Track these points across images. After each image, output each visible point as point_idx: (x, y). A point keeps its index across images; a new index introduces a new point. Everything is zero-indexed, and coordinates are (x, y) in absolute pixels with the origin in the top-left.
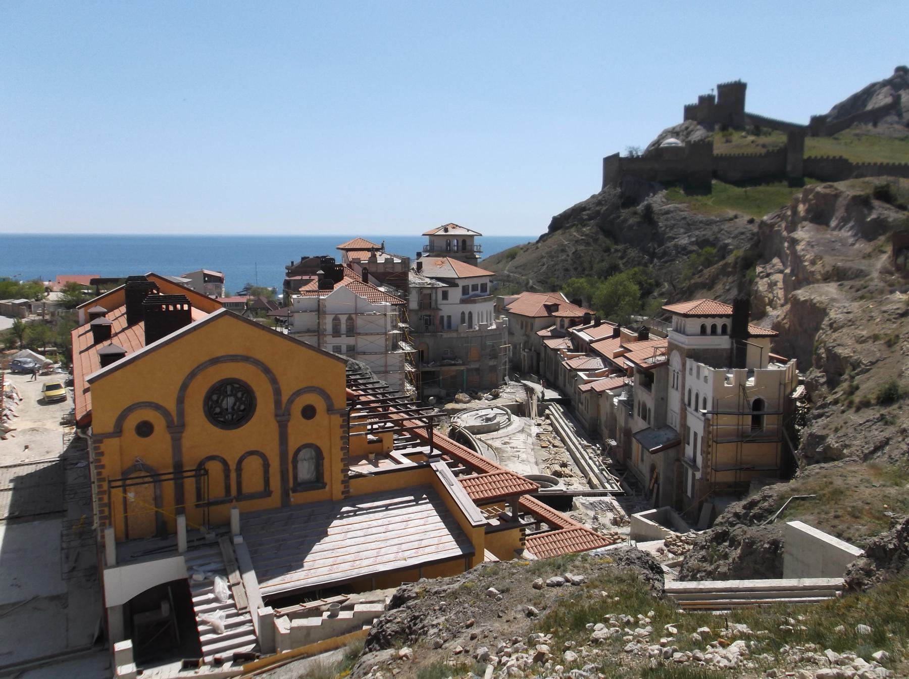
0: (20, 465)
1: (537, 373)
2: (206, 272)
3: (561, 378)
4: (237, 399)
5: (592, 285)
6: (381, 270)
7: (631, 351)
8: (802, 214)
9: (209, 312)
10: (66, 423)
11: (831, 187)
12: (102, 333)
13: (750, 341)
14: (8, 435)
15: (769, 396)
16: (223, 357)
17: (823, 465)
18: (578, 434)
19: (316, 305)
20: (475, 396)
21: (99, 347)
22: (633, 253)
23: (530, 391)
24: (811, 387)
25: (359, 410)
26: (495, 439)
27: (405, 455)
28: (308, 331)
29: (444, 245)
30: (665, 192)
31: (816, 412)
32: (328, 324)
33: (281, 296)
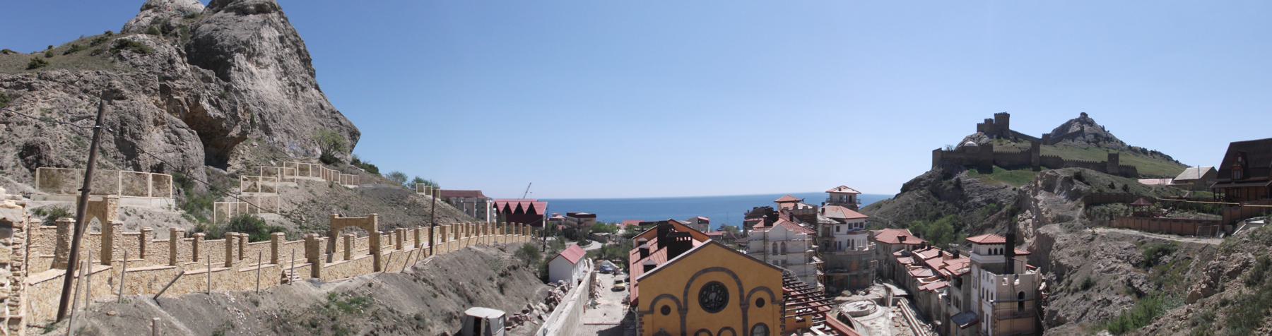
0: (601, 324)
1: (893, 278)
2: (700, 217)
3: (907, 282)
4: (718, 294)
5: (926, 225)
6: (801, 213)
7: (948, 265)
8: (1040, 186)
9: (702, 242)
10: (625, 303)
11: (1053, 172)
12: (645, 253)
13: (1016, 258)
14: (597, 307)
15: (1027, 290)
16: (710, 268)
18: (918, 317)
19: (762, 235)
20: (854, 292)
21: (643, 261)
22: (950, 206)
23: (888, 290)
24: (1049, 282)
25: (790, 301)
26: (866, 320)
27: (820, 329)
28: (758, 252)
29: (838, 198)
30: (967, 171)
31: (1052, 297)
32: (770, 247)
33: (742, 231)
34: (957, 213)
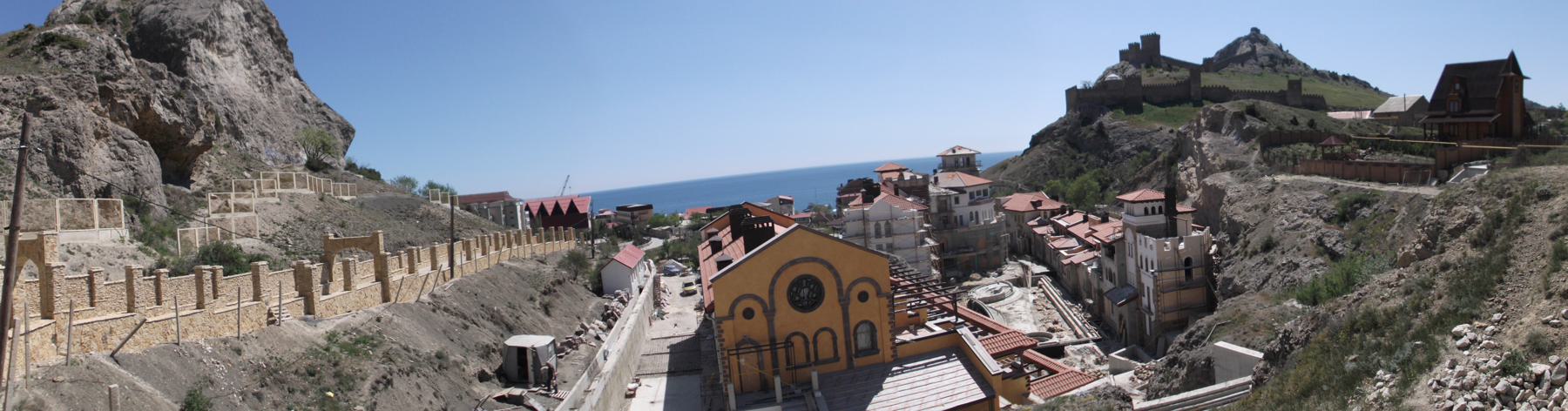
1: (1030, 254)
2: (781, 197)
3: (1048, 257)
4: (811, 290)
5: (1065, 185)
6: (908, 185)
7: (1096, 231)
8: (1204, 125)
9: (787, 227)
10: (698, 309)
11: (1220, 106)
12: (717, 247)
13: (1179, 217)
15: (1195, 256)
16: (798, 259)
17: (1233, 299)
18: (1064, 297)
19: (861, 215)
20: (984, 274)
21: (716, 256)
22: (1092, 158)
23: (1025, 268)
24: (1220, 244)
25: (899, 293)
26: (1001, 306)
27: (937, 324)
28: (857, 235)
29: (953, 162)
30: (1111, 113)
31: (1225, 262)
32: (872, 228)
33: (835, 210)
34: (1102, 167)
